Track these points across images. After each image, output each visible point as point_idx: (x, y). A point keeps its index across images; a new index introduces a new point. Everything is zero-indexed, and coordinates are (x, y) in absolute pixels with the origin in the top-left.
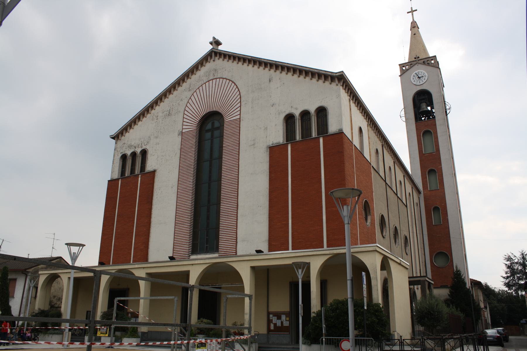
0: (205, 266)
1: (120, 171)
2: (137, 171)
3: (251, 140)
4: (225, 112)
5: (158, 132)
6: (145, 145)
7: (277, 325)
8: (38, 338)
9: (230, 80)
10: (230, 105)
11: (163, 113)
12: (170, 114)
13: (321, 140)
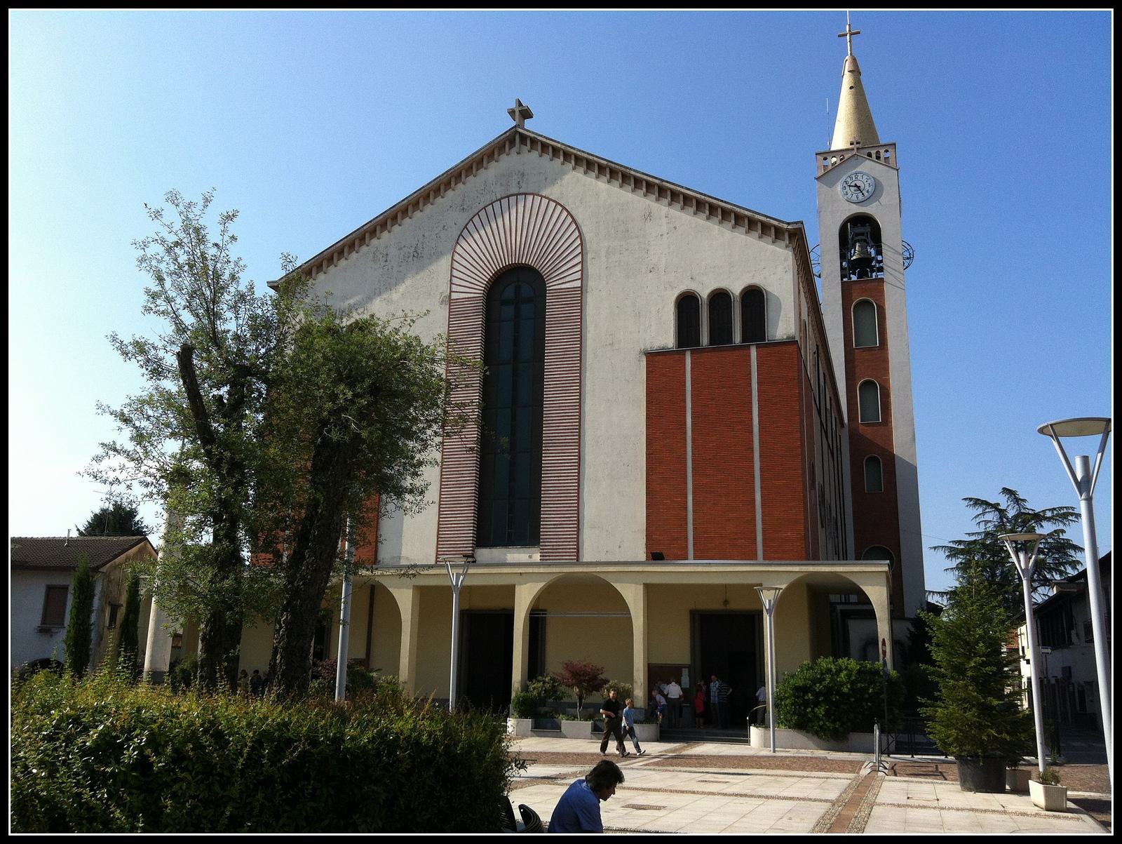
13: (754, 352)
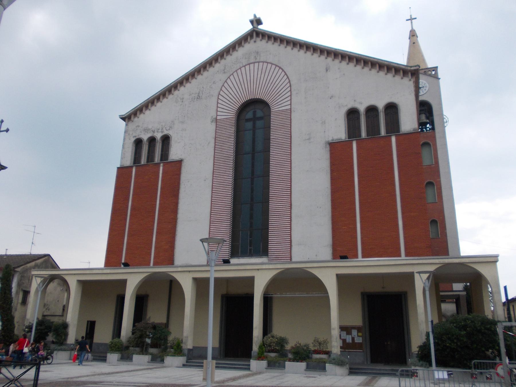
0: (275, 272)
1: (133, 158)
2: (157, 158)
3: (306, 134)
4: (272, 100)
5: (184, 116)
6: (167, 130)
7: (346, 341)
8: (52, 357)
9: (276, 66)
10: (278, 93)
11: (190, 95)
12: (200, 97)
13: (393, 139)
